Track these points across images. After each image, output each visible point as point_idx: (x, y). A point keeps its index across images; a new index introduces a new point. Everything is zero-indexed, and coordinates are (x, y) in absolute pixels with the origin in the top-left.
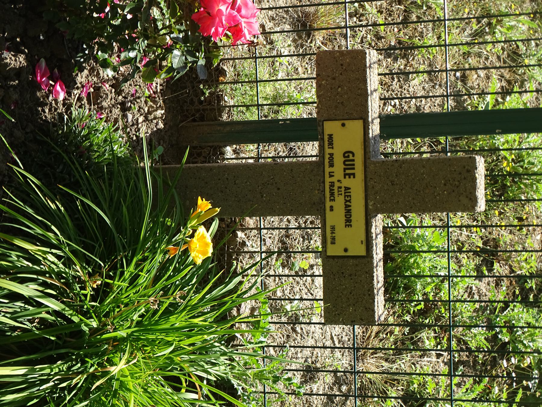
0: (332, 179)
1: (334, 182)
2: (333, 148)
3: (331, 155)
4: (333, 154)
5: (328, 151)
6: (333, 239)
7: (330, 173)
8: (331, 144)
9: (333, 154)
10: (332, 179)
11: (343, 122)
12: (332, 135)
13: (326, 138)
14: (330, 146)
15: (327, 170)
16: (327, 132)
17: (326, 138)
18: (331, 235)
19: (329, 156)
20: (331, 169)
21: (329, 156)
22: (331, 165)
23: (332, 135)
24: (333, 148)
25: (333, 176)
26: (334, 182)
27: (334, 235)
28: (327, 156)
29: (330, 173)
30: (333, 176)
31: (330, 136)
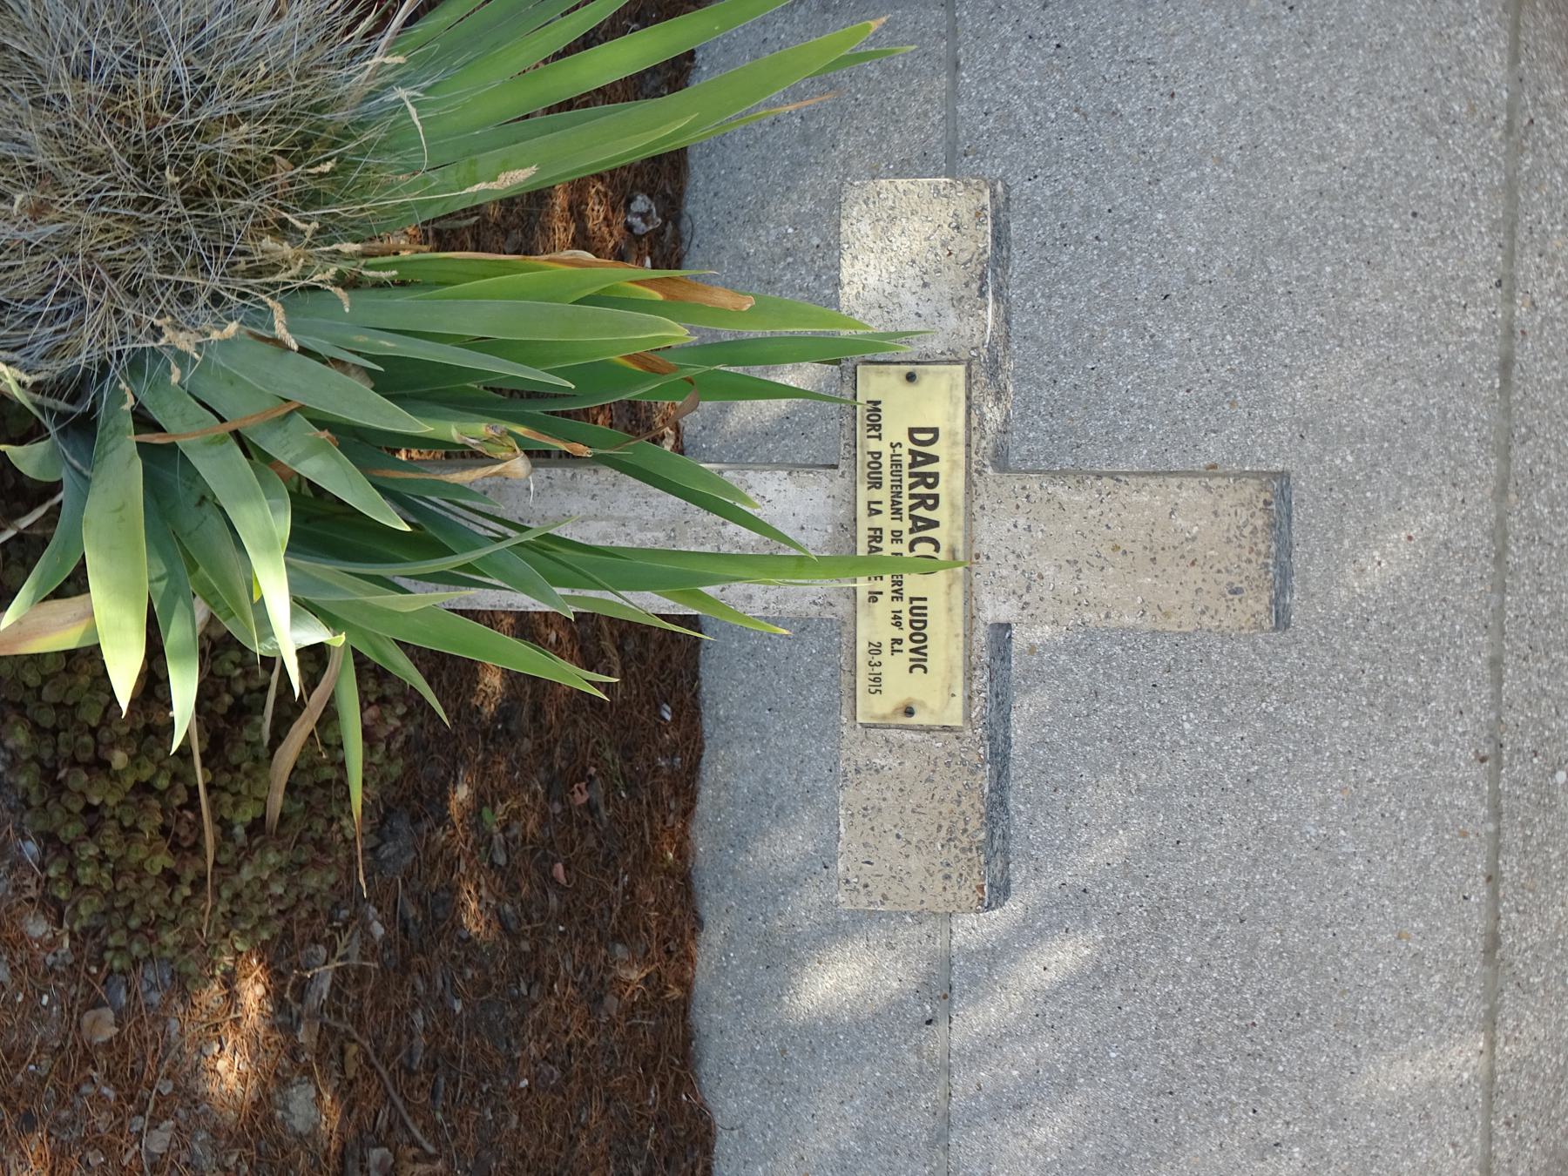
0: (877, 521)
2: (879, 437)
6: (877, 679)
7: (870, 503)
8: (875, 426)
10: (877, 521)
11: (909, 368)
14: (873, 433)
19: (870, 458)
21: (870, 458)
22: (876, 484)
24: (879, 437)
25: (879, 512)
27: (877, 670)
29: (870, 503)
30: (879, 512)
31: (875, 406)
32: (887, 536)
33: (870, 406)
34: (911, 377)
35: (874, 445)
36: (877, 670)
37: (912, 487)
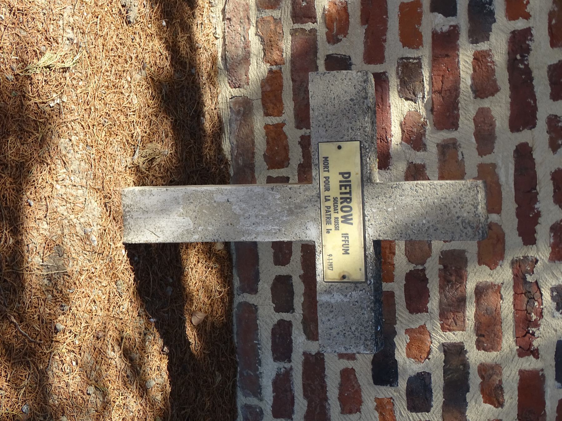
1: (330, 207)
2: (328, 171)
3: (327, 178)
4: (329, 177)
5: (323, 174)
7: (326, 197)
8: (326, 167)
9: (329, 177)
12: (328, 158)
13: (322, 160)
14: (326, 169)
15: (323, 194)
16: (323, 154)
17: (322, 160)
18: (328, 261)
20: (327, 193)
21: (325, 179)
22: (327, 189)
23: (328, 158)
24: (328, 171)
25: (329, 200)
26: (330, 207)
28: (322, 180)
30: (329, 200)
31: (326, 159)
32: (332, 209)
33: (323, 159)
34: (339, 147)
35: (326, 174)
36: (331, 261)
37: (341, 203)
